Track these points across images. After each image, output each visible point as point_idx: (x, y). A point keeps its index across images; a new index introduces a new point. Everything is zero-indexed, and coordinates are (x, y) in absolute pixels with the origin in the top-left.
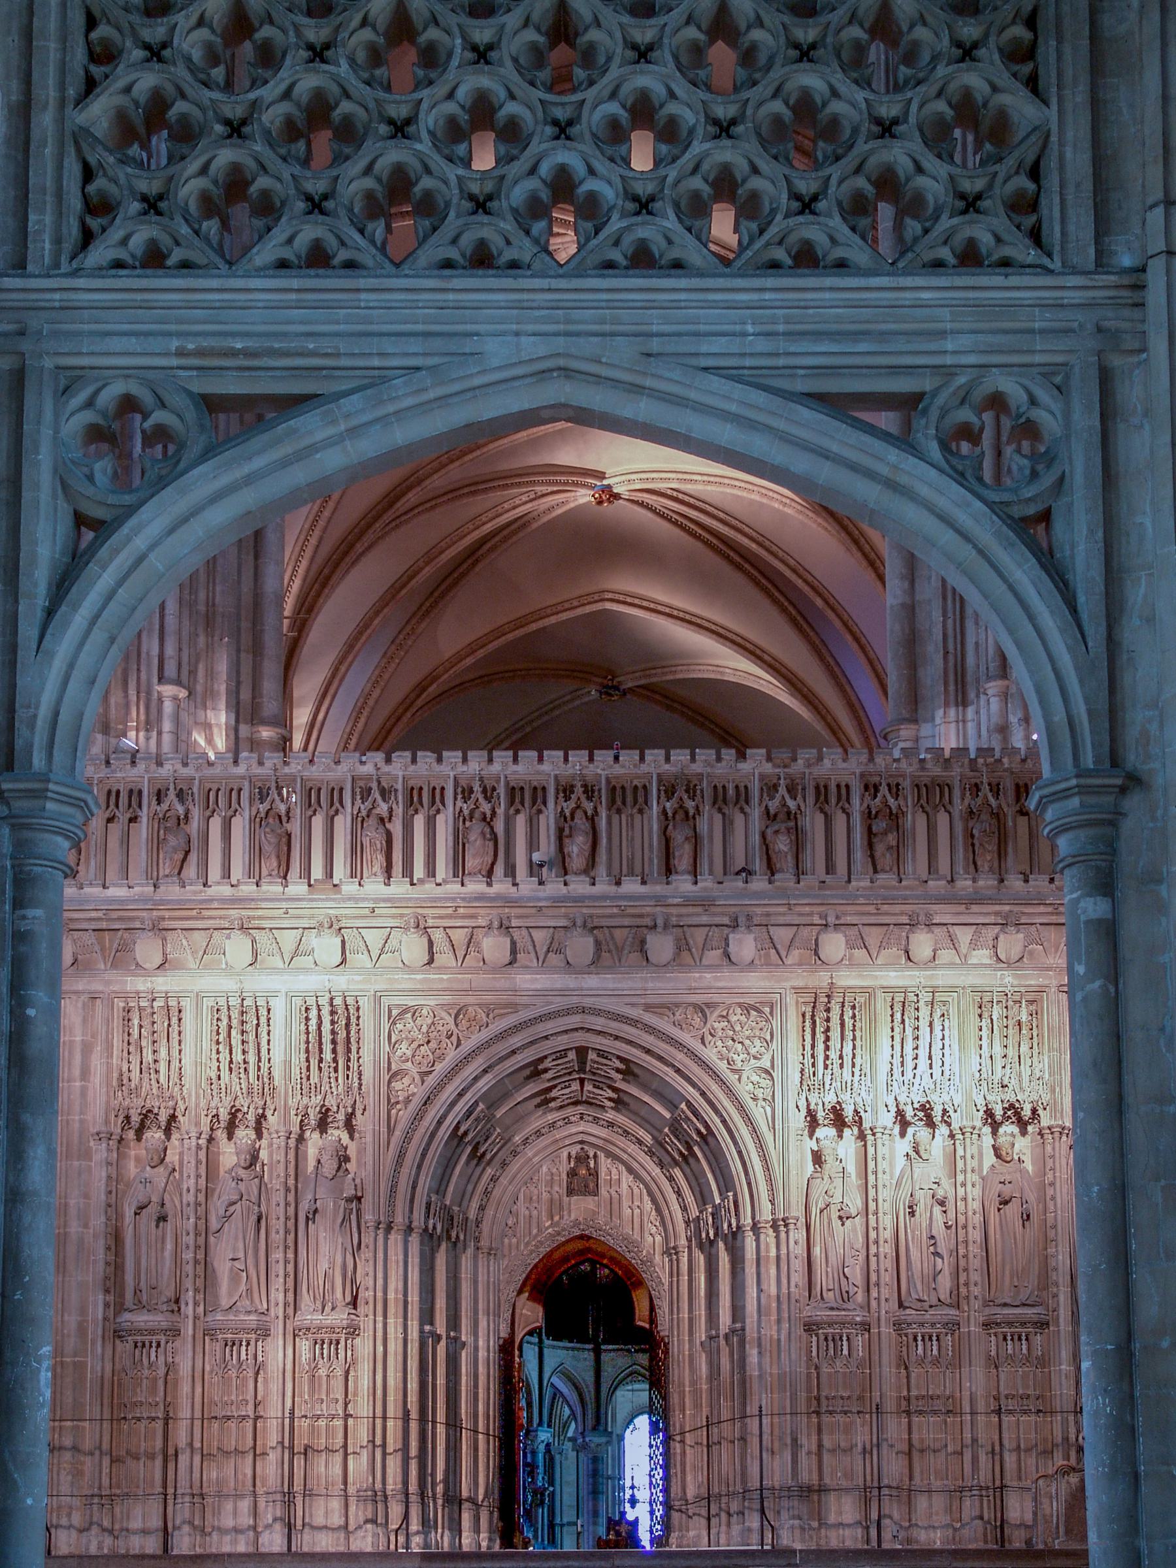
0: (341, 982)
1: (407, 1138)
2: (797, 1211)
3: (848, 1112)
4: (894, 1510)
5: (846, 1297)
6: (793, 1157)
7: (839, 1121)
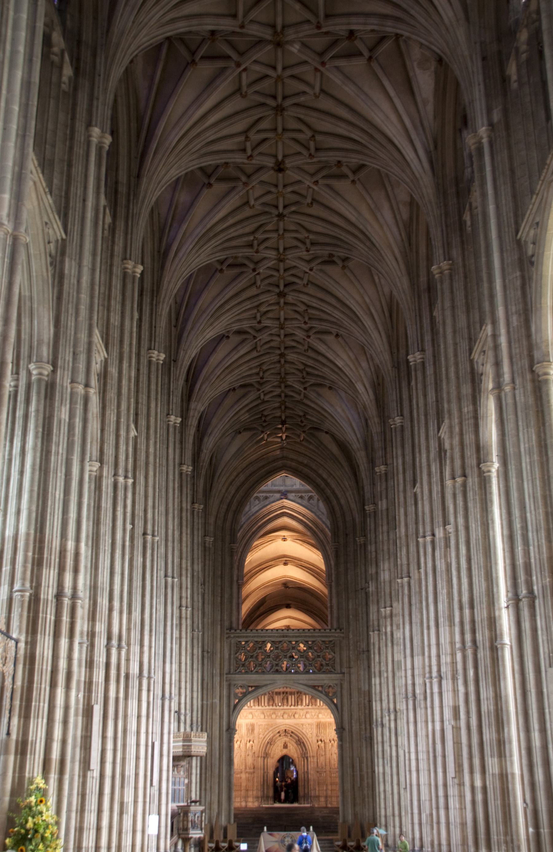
0: (253, 721)
2: (315, 755)
4: (329, 799)
7: (321, 741)
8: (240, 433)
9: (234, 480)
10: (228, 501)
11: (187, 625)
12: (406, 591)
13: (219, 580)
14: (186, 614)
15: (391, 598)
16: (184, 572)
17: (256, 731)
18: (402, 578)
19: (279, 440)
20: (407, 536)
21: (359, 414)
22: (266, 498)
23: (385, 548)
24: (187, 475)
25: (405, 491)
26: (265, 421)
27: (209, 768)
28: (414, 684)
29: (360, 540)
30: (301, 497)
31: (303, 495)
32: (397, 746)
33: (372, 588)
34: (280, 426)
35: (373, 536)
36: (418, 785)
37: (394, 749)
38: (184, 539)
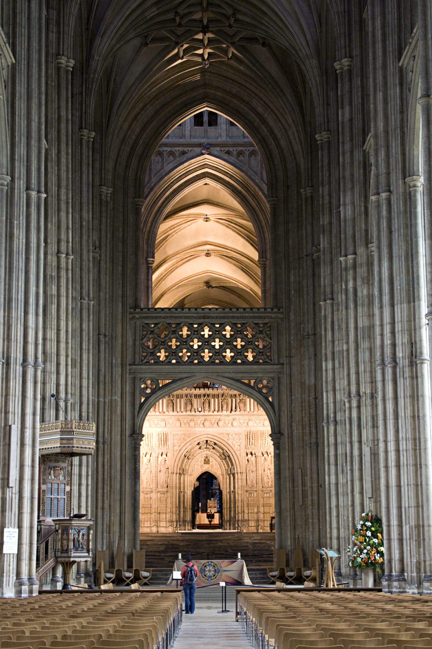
0: (165, 430)
1: (176, 457)
2: (244, 471)
3: (253, 453)
4: (261, 524)
5: (253, 486)
6: (244, 461)
7: (252, 454)
8: (147, 44)
9: (139, 114)
10: (131, 142)
11: (67, 279)
12: (384, 213)
13: (120, 244)
14: (67, 263)
15: (354, 242)
16: (63, 206)
17: (170, 442)
18: (378, 194)
19: (200, 60)
20: (386, 132)
21: (309, 6)
22: (184, 153)
23: (348, 174)
24: (67, 71)
25: (385, 66)
26: (180, 25)
27: (107, 482)
28: (394, 345)
29: (305, 192)
30: (228, 153)
31: (231, 149)
32: (360, 442)
33: (324, 243)
34: (200, 36)
35: (326, 174)
36: (399, 486)
37: (356, 446)
38: (63, 160)
